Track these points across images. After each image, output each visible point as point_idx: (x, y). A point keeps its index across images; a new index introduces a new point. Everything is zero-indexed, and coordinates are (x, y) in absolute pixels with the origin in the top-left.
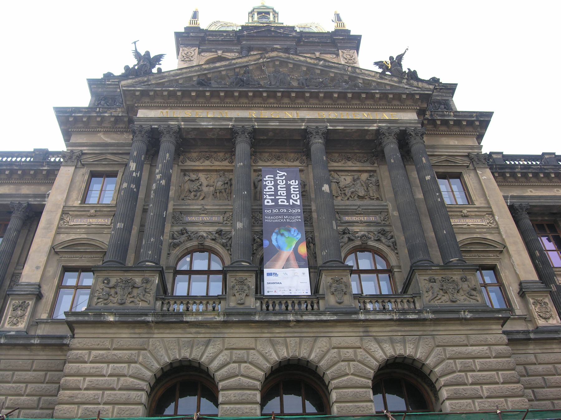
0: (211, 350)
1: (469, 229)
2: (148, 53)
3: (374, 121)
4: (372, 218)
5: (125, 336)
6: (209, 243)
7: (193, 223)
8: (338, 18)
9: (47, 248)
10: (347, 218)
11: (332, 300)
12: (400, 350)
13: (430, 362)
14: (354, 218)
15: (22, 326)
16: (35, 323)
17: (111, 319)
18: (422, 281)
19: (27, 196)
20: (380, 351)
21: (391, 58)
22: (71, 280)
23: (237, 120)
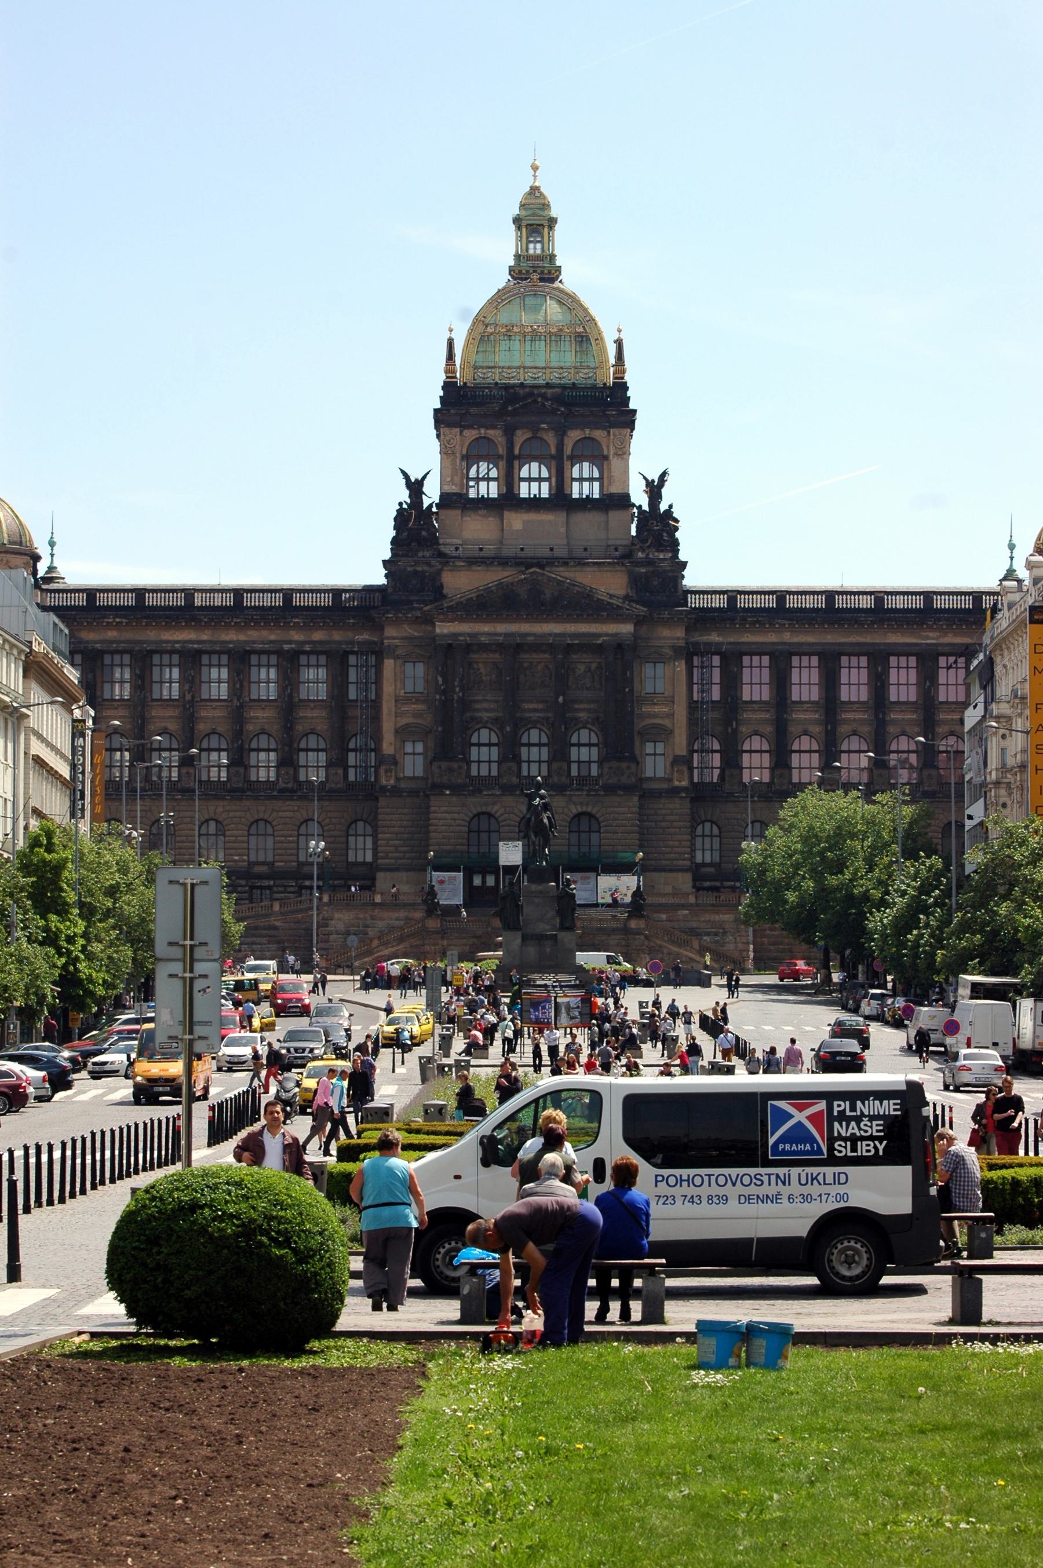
0: (496, 808)
1: (655, 716)
2: (416, 480)
3: (600, 635)
4: (592, 706)
5: (454, 799)
6: (489, 725)
7: (477, 710)
8: (619, 343)
9: (393, 730)
10: (576, 706)
11: (555, 779)
12: (585, 809)
13: (598, 815)
14: (582, 706)
15: (392, 782)
16: (398, 779)
17: (448, 792)
18: (606, 765)
19: (340, 643)
20: (575, 810)
21: (653, 481)
22: (409, 748)
23: (506, 635)
